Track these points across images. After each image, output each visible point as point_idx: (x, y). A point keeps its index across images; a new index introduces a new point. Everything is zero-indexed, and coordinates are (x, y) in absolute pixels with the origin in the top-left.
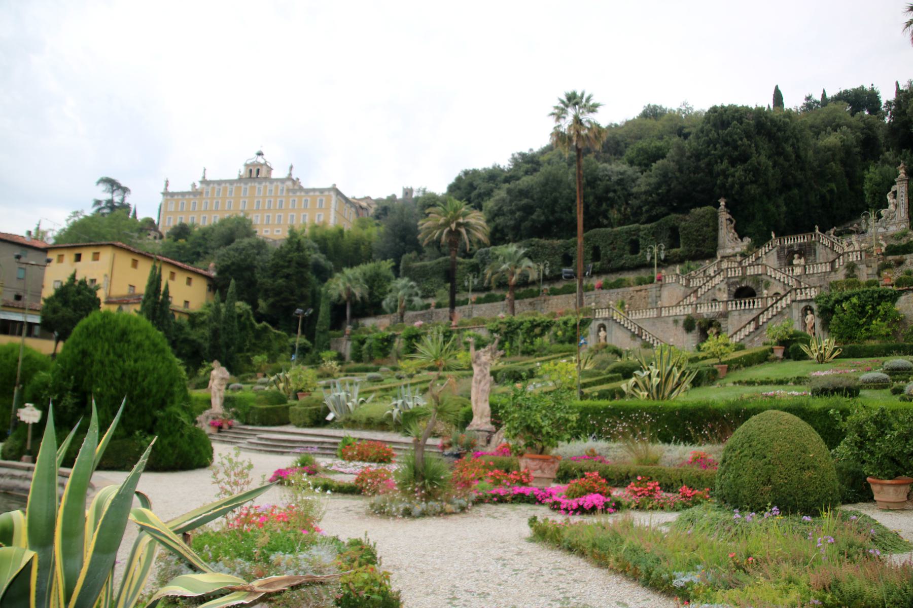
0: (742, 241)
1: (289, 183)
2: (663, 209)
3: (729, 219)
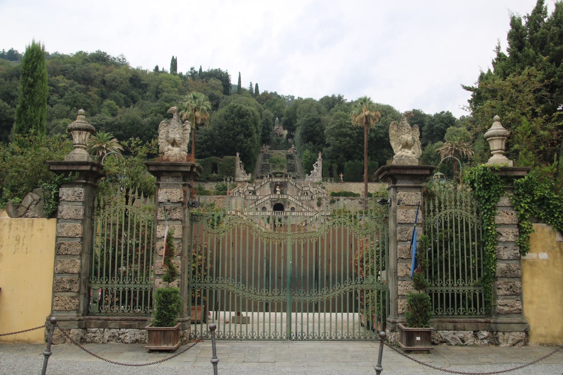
0: (248, 175)
2: (208, 153)
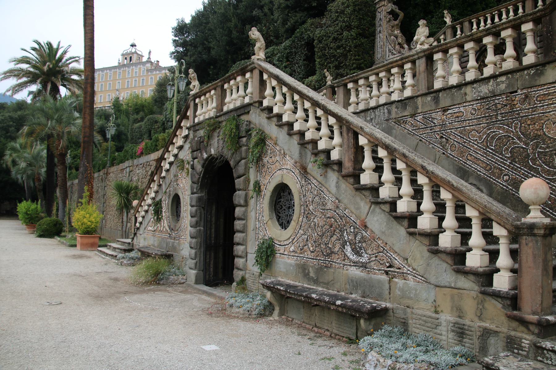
1: (149, 65)
3: (392, 13)
